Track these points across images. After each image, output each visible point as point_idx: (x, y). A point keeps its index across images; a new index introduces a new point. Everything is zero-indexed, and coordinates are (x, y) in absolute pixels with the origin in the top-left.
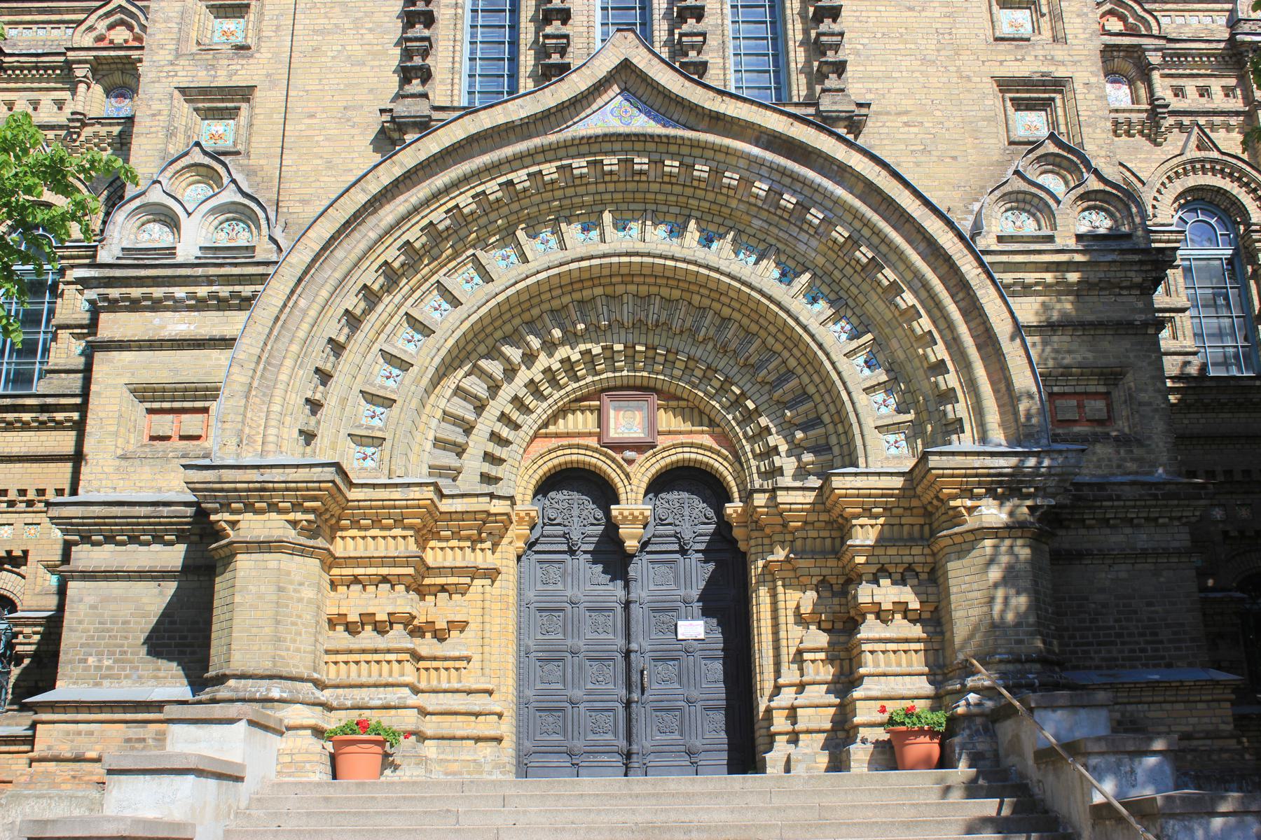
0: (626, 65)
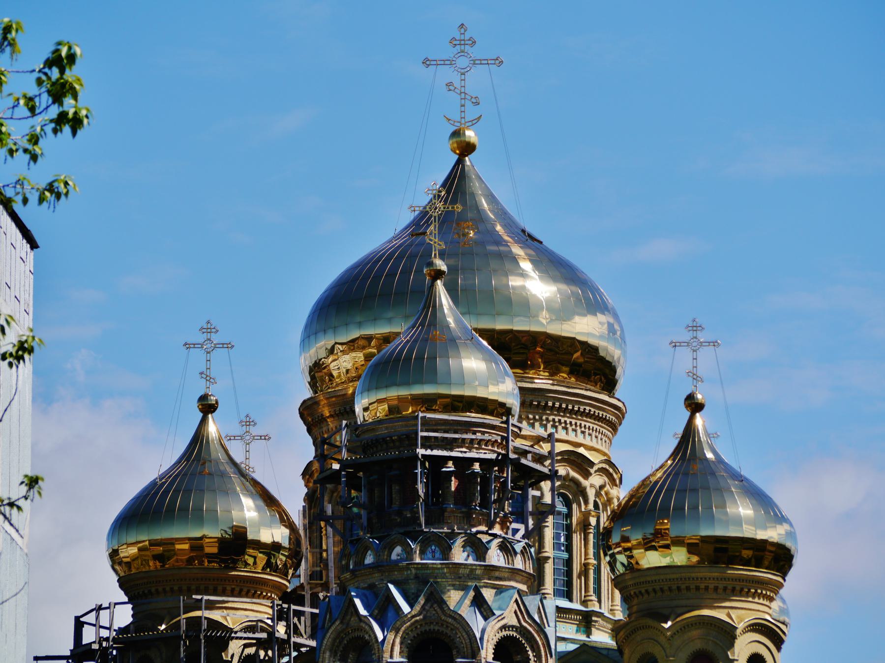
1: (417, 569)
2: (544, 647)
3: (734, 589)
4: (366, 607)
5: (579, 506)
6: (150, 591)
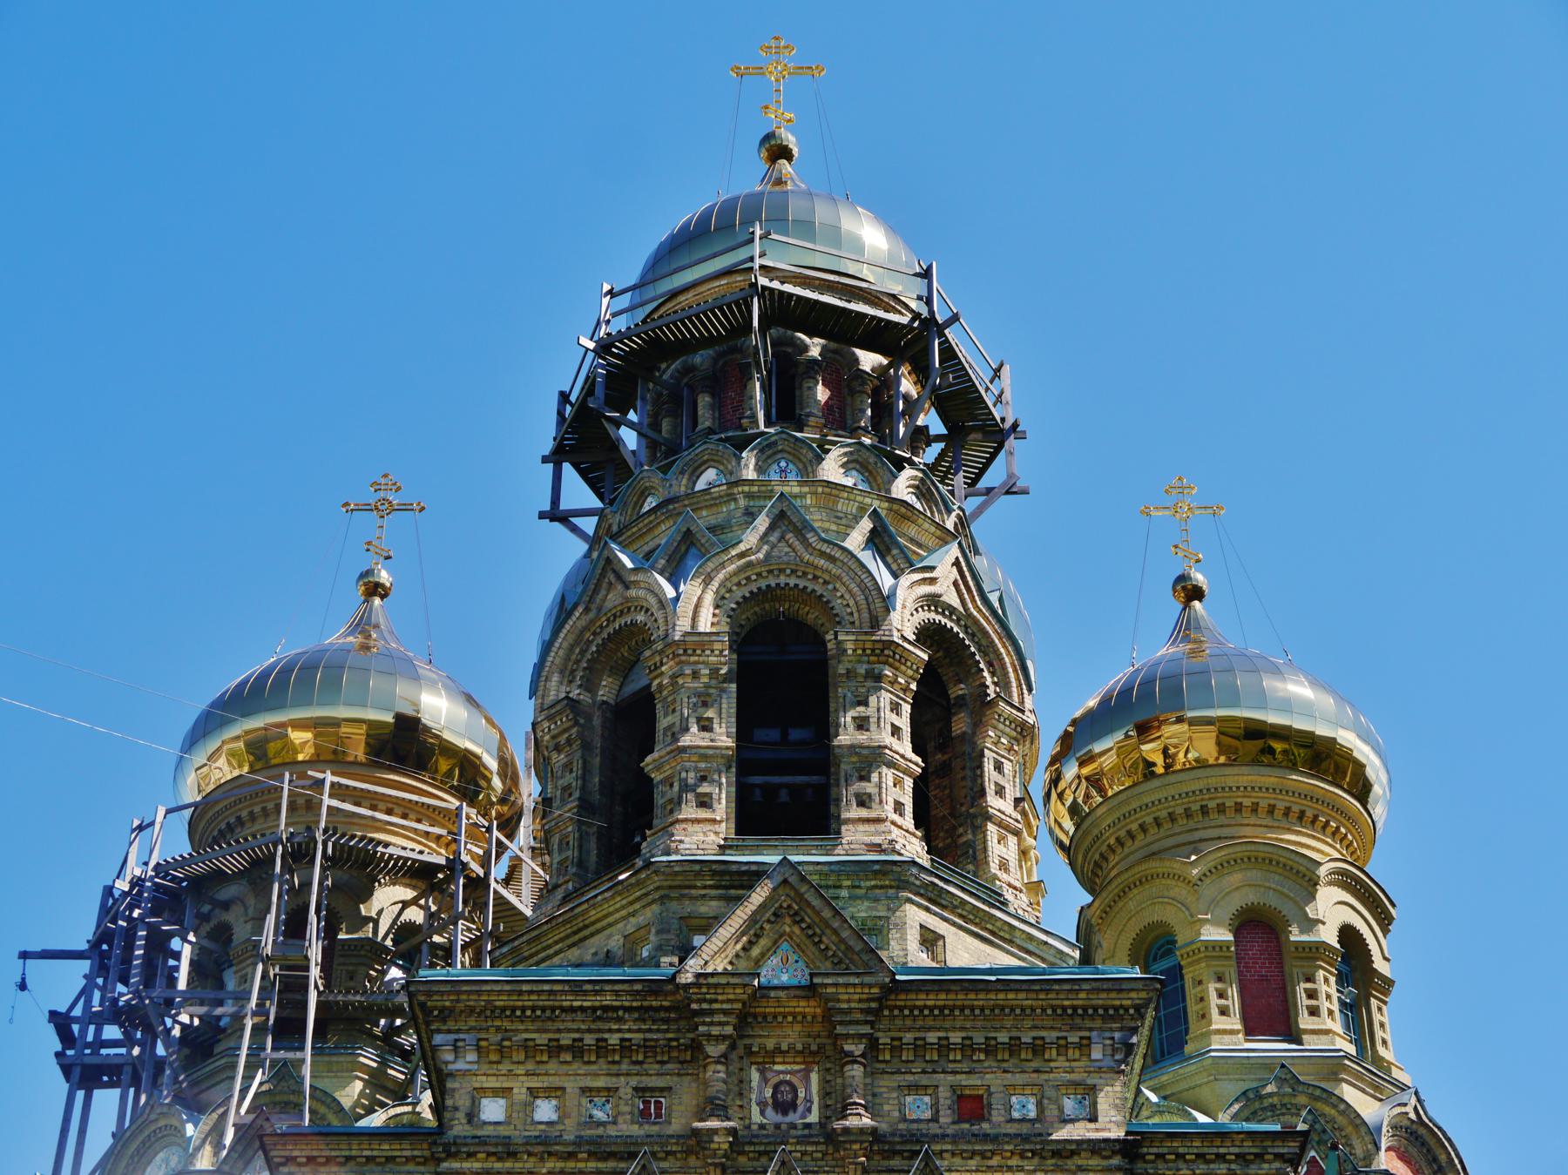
2: (1015, 670)
6: (239, 818)
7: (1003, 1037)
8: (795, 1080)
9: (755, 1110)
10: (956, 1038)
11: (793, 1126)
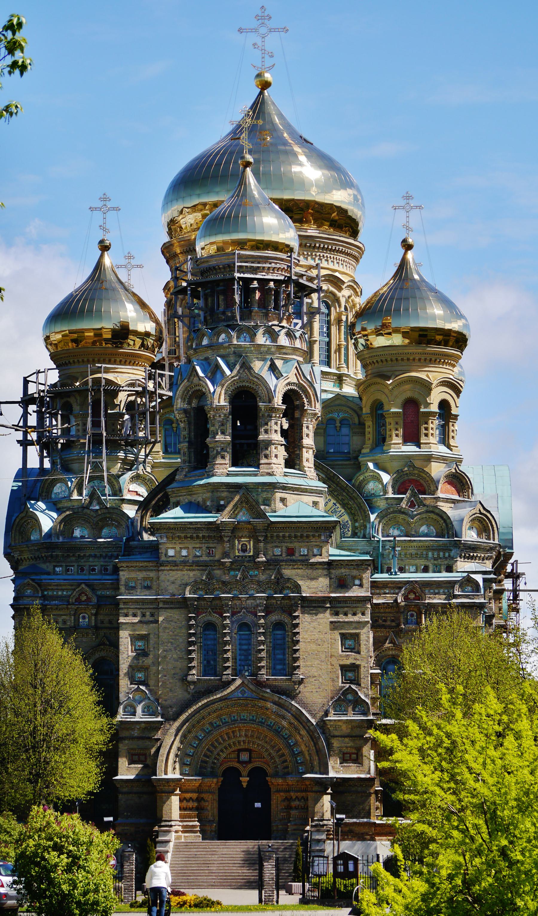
0: (243, 682)
1: (235, 348)
3: (431, 360)
4: (204, 371)
5: (336, 308)
6: (69, 362)
7: (299, 534)
8: (247, 543)
9: (237, 551)
10: (287, 534)
11: (246, 556)
